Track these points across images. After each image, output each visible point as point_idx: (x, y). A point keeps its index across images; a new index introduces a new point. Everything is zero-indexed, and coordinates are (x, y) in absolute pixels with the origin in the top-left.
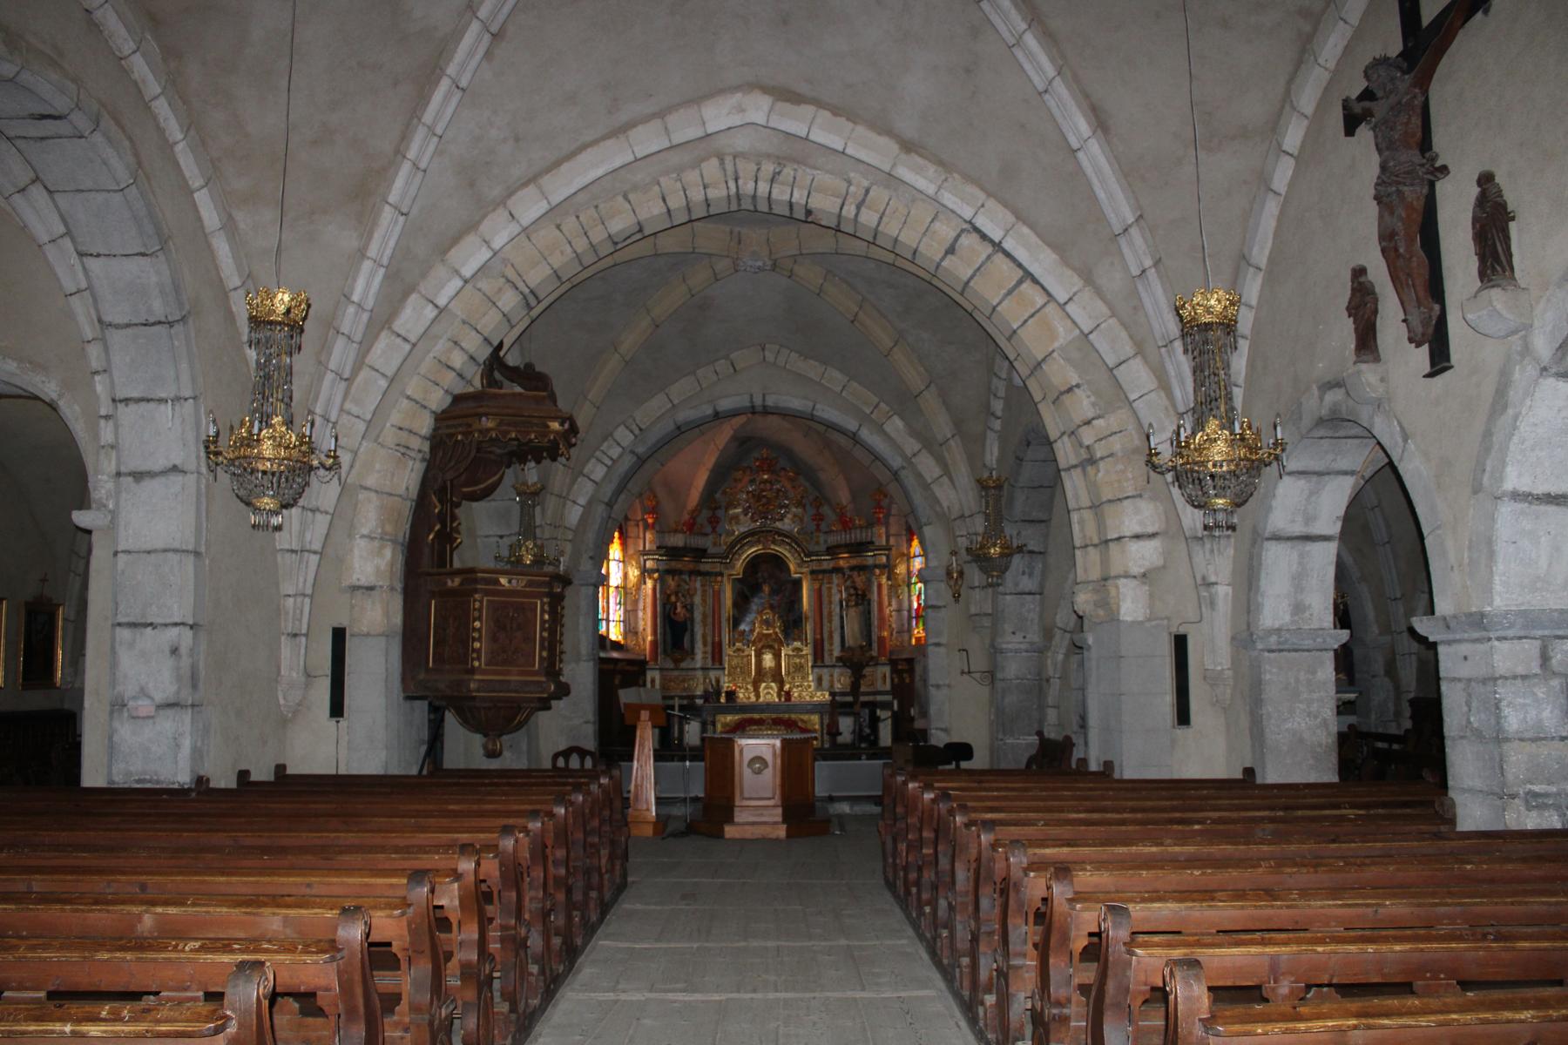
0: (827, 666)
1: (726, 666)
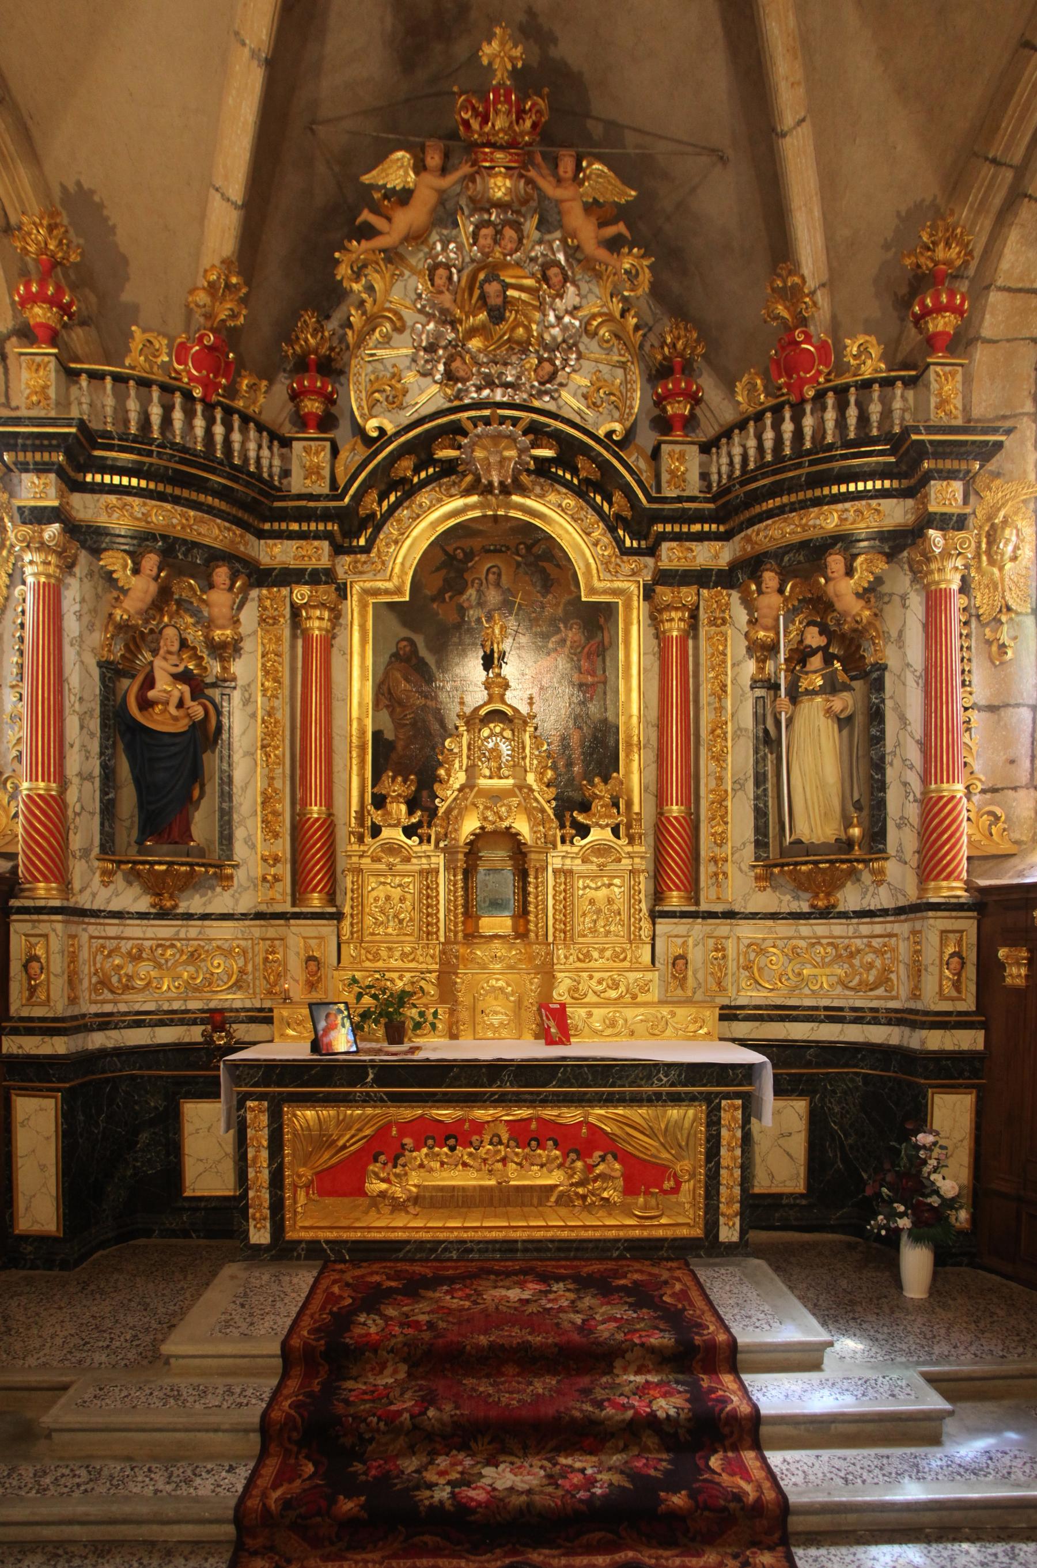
1: (347, 910)
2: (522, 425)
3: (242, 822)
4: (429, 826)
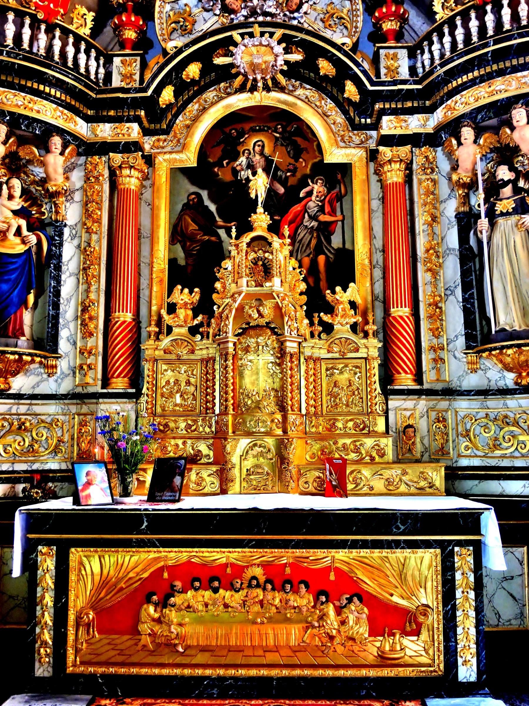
0: (430, 392)
3: (65, 326)
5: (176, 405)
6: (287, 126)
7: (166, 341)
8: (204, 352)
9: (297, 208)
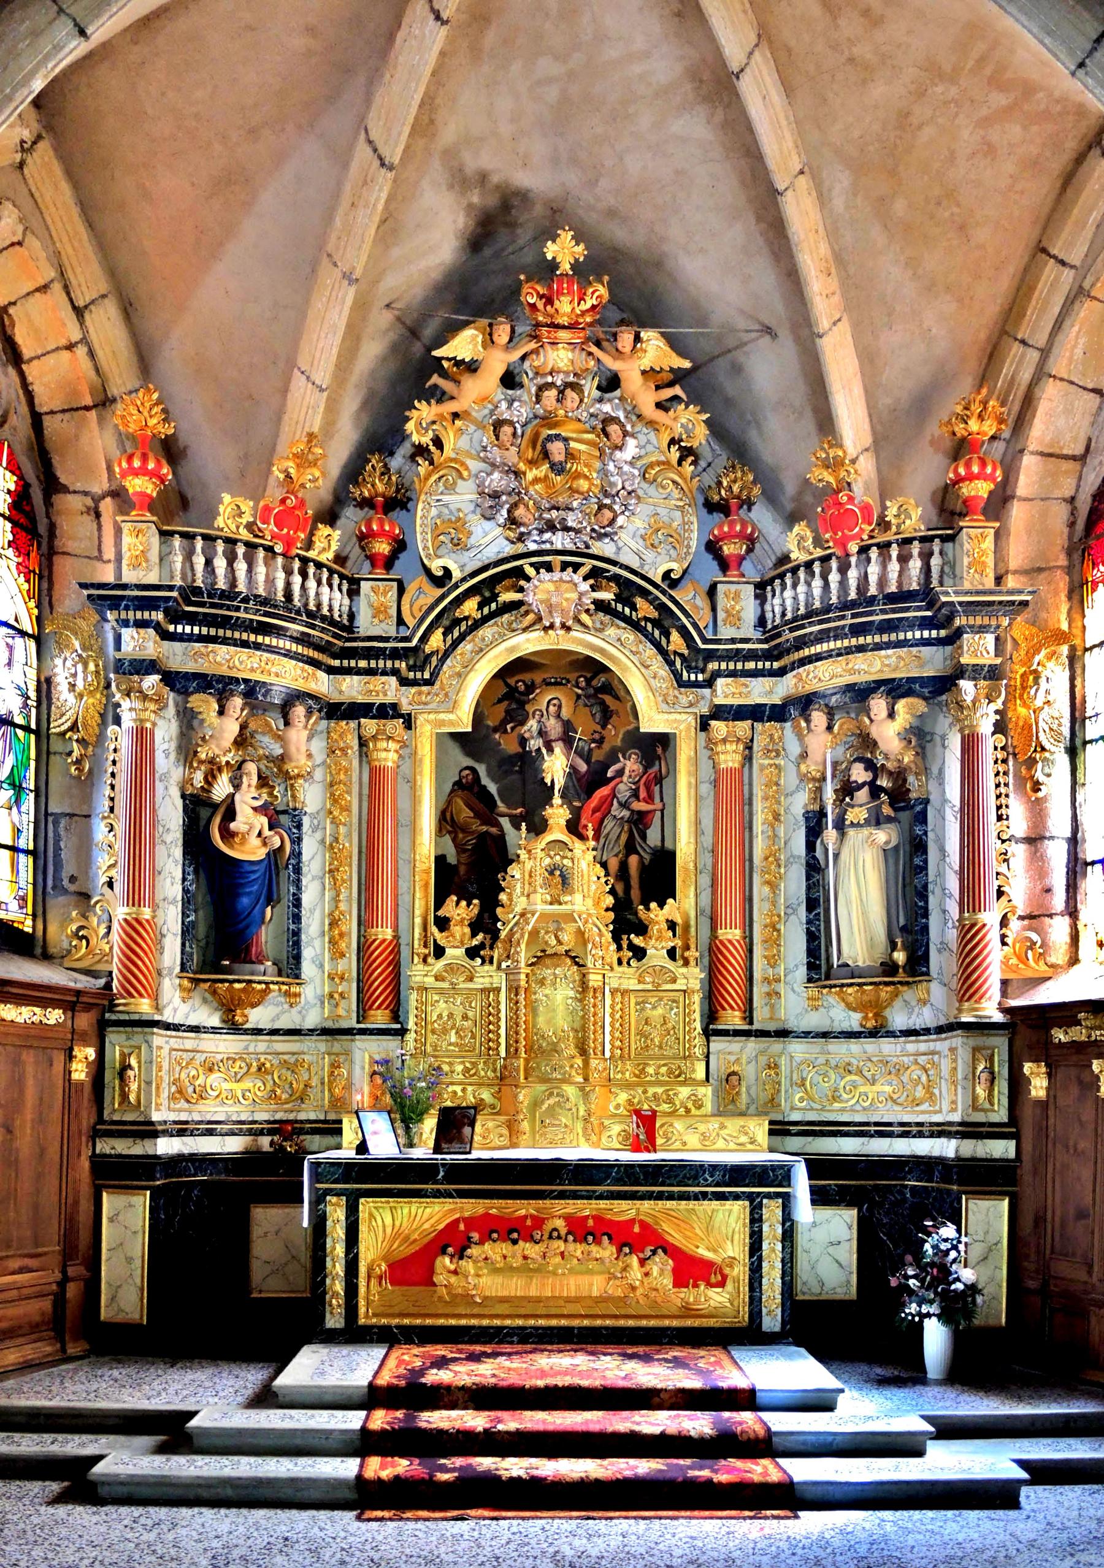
1: (411, 1025)
2: (583, 571)
3: (308, 944)
4: (492, 948)
5: (450, 1044)
6: (593, 678)
7: (440, 964)
8: (487, 980)
9: (604, 791)
